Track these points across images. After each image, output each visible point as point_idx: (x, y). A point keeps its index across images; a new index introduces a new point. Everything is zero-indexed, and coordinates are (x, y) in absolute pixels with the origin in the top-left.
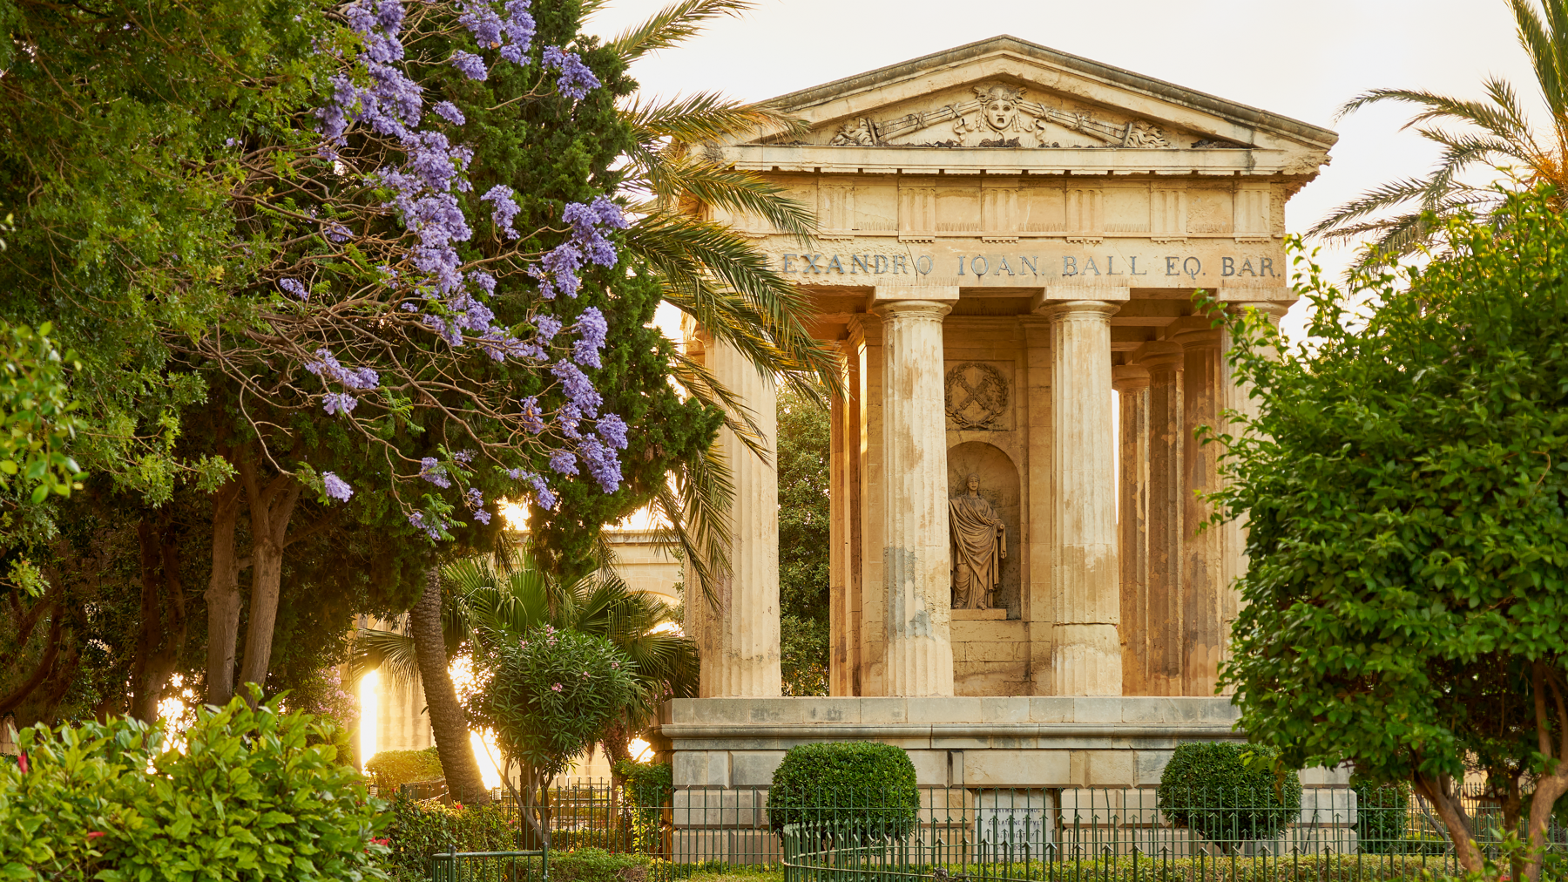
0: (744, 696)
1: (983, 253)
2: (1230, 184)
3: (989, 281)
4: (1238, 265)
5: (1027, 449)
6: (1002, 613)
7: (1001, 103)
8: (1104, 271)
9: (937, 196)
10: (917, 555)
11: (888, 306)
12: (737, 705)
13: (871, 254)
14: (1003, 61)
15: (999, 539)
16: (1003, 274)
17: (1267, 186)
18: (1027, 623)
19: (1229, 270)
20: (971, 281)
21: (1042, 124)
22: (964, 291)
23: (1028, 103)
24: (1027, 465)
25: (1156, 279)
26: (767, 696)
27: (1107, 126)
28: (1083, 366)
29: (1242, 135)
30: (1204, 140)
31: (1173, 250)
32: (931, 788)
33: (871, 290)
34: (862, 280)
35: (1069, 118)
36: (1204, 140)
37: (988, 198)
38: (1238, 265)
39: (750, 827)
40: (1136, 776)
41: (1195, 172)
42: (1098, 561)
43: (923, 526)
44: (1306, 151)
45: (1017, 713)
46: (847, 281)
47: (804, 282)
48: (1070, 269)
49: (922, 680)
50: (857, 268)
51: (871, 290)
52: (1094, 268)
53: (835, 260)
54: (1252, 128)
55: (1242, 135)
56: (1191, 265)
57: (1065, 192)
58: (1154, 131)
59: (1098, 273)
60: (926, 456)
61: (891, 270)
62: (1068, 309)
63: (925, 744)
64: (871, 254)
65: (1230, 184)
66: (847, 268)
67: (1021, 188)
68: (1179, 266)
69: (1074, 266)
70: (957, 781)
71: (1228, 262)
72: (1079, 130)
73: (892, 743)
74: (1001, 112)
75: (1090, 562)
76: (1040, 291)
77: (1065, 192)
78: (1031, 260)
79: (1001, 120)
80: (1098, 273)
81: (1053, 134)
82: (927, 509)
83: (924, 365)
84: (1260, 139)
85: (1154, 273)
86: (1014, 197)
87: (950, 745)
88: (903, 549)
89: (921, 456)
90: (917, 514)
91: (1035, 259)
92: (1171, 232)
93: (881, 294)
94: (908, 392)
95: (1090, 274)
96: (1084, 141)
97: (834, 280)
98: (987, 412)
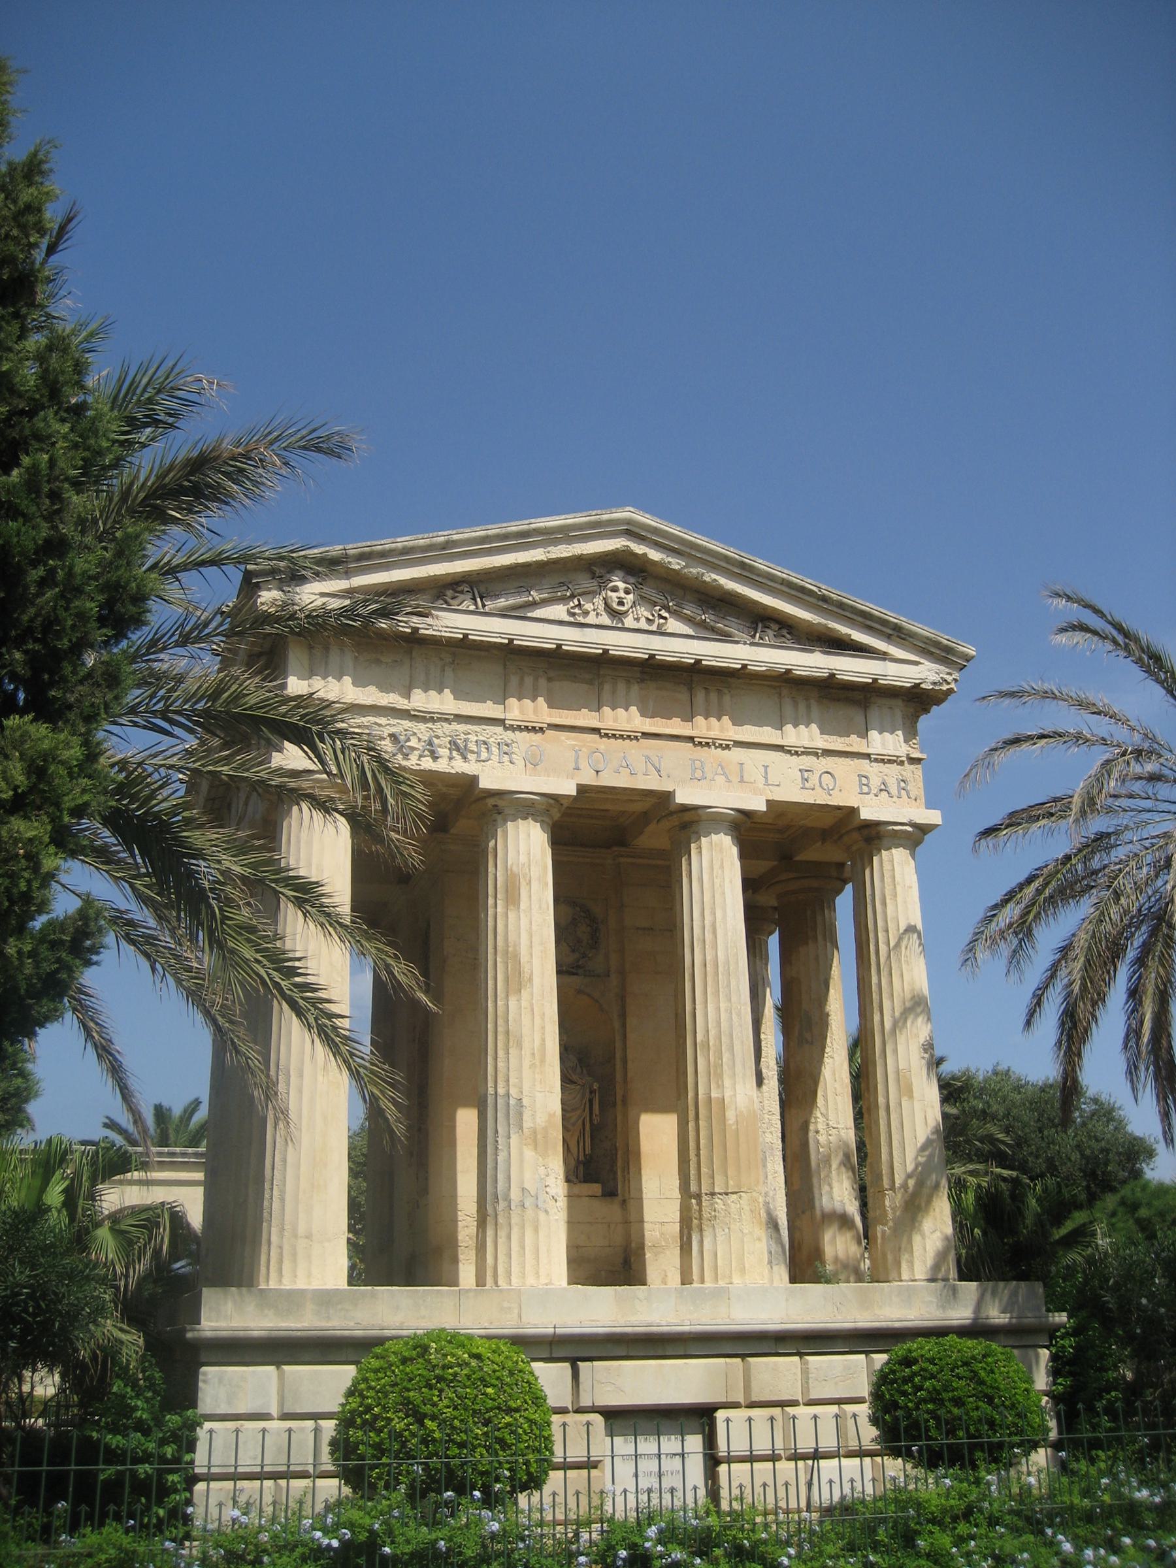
0: (301, 1285)
1: (602, 747)
3: (609, 779)
4: (875, 783)
5: (622, 998)
6: (596, 1188)
8: (735, 779)
9: (550, 680)
10: (525, 1102)
11: (491, 802)
12: (293, 1299)
13: (473, 738)
15: (591, 1101)
17: (899, 702)
18: (624, 1202)
19: (865, 789)
20: (589, 779)
22: (582, 789)
23: (648, 591)
24: (623, 1015)
25: (792, 792)
26: (330, 1286)
28: (715, 882)
33: (474, 779)
34: (460, 766)
37: (607, 687)
38: (875, 783)
39: (303, 1475)
40: (805, 1388)
41: (832, 675)
43: (533, 1066)
46: (442, 766)
48: (698, 774)
49: (520, 1272)
50: (455, 753)
51: (474, 779)
52: (724, 774)
53: (430, 743)
56: (826, 779)
57: (691, 689)
58: (784, 632)
59: (729, 781)
60: (536, 980)
61: (495, 758)
64: (473, 738)
66: (443, 752)
67: (643, 680)
68: (814, 779)
69: (702, 769)
70: (585, 1402)
71: (864, 781)
74: (622, 594)
75: (731, 1115)
76: (668, 796)
77: (691, 689)
78: (655, 760)
79: (621, 603)
80: (729, 781)
82: (537, 1043)
83: (535, 872)
86: (635, 688)
87: (577, 1350)
88: (508, 1095)
89: (531, 979)
90: (526, 1052)
91: (660, 758)
93: (485, 783)
95: (720, 779)
97: (428, 764)
98: (577, 955)
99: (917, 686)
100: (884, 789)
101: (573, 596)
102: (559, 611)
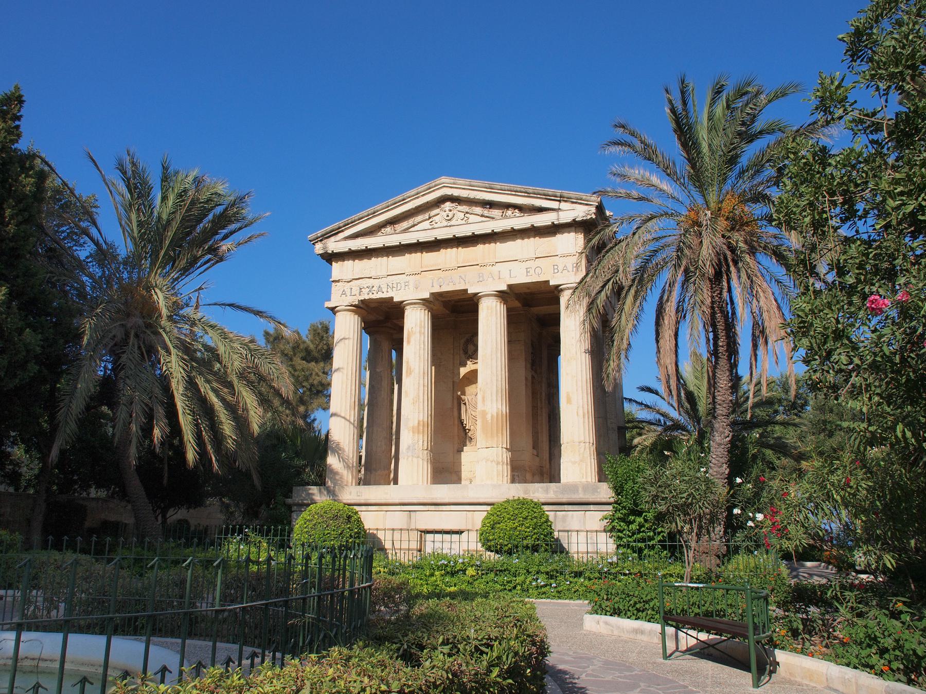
2: (554, 229)
4: (560, 269)
7: (447, 209)
14: (445, 189)
16: (450, 284)
20: (437, 289)
21: (467, 215)
23: (460, 208)
27: (496, 213)
29: (554, 205)
30: (541, 210)
31: (528, 264)
32: (401, 530)
33: (392, 298)
35: (478, 210)
36: (541, 210)
38: (560, 269)
42: (492, 416)
44: (586, 208)
45: (444, 492)
47: (367, 297)
51: (392, 298)
54: (559, 201)
55: (554, 205)
62: (481, 297)
63: (398, 508)
65: (554, 229)
66: (384, 290)
68: (532, 272)
72: (482, 216)
73: (357, 508)
75: (489, 417)
81: (472, 218)
84: (563, 205)
85: (521, 276)
92: (526, 256)
94: (409, 342)
96: (484, 219)
97: (380, 295)
99: (574, 220)
100: (565, 268)
101: (430, 218)
102: (426, 225)
